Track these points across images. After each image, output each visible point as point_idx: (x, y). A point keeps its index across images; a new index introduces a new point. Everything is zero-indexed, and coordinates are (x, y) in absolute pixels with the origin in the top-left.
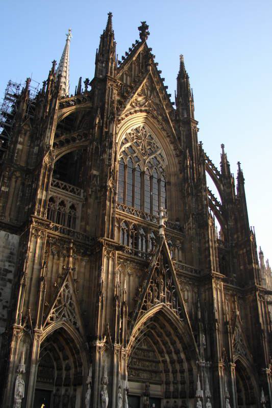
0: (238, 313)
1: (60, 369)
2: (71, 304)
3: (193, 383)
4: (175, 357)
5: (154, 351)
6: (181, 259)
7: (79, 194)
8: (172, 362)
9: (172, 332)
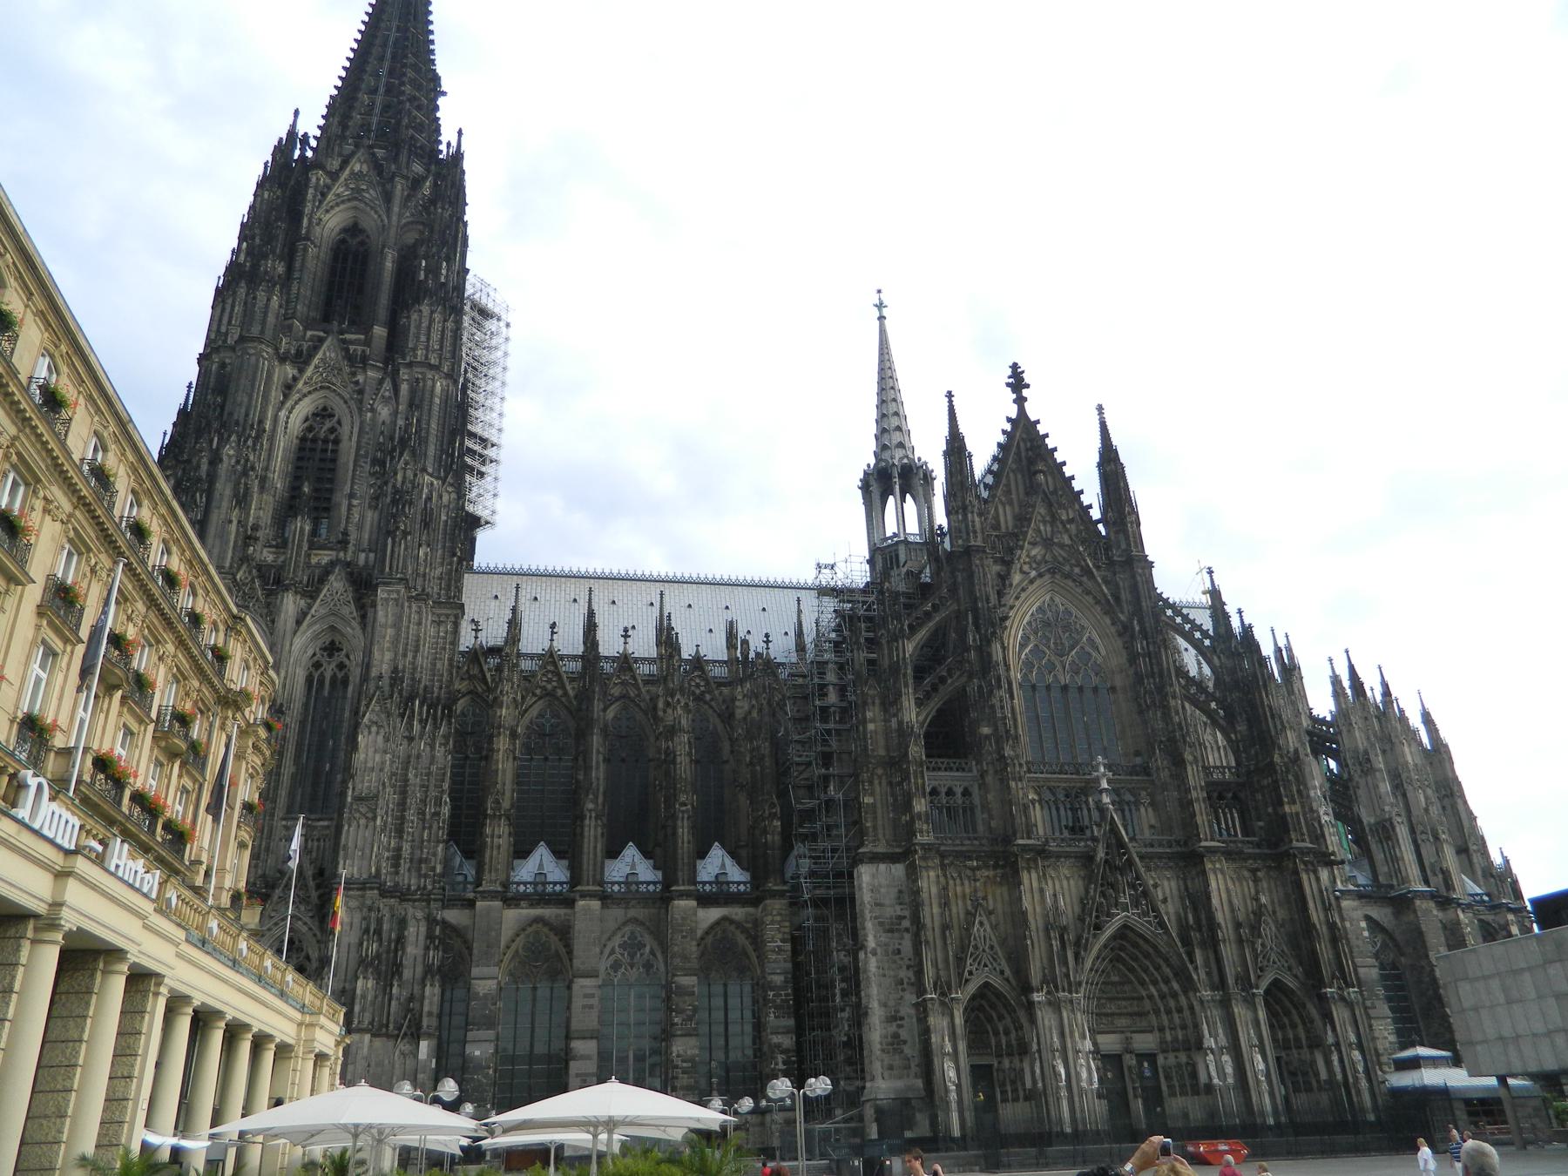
0: (1263, 900)
1: (996, 1033)
2: (992, 947)
3: (1197, 1026)
4: (1164, 988)
5: (1131, 982)
6: (1153, 822)
7: (970, 770)
8: (1163, 997)
9: (1151, 951)
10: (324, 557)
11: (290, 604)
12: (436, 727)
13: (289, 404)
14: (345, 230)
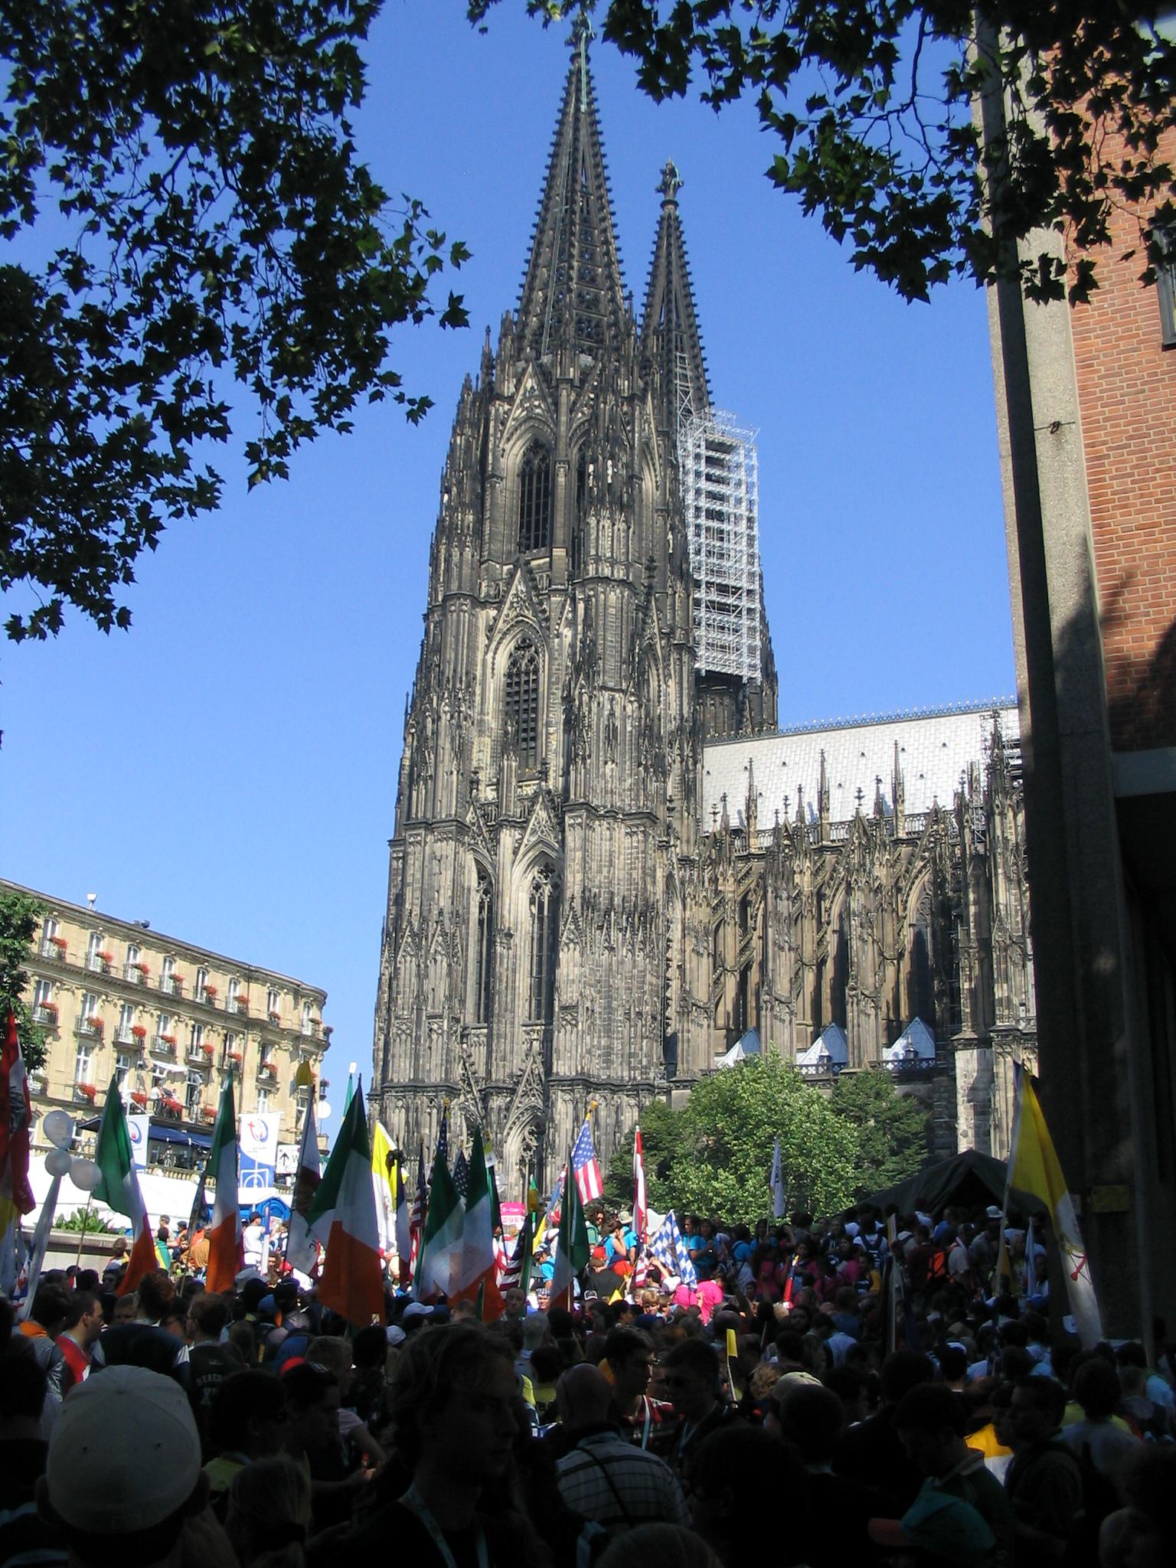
10: (529, 790)
11: (507, 838)
12: (634, 934)
13: (493, 647)
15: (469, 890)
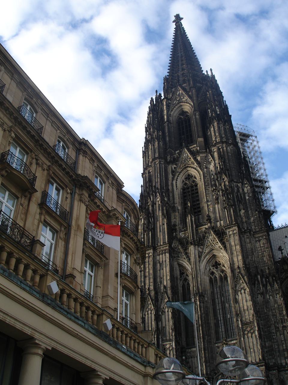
12: (272, 286)
14: (180, 114)
15: (177, 278)
